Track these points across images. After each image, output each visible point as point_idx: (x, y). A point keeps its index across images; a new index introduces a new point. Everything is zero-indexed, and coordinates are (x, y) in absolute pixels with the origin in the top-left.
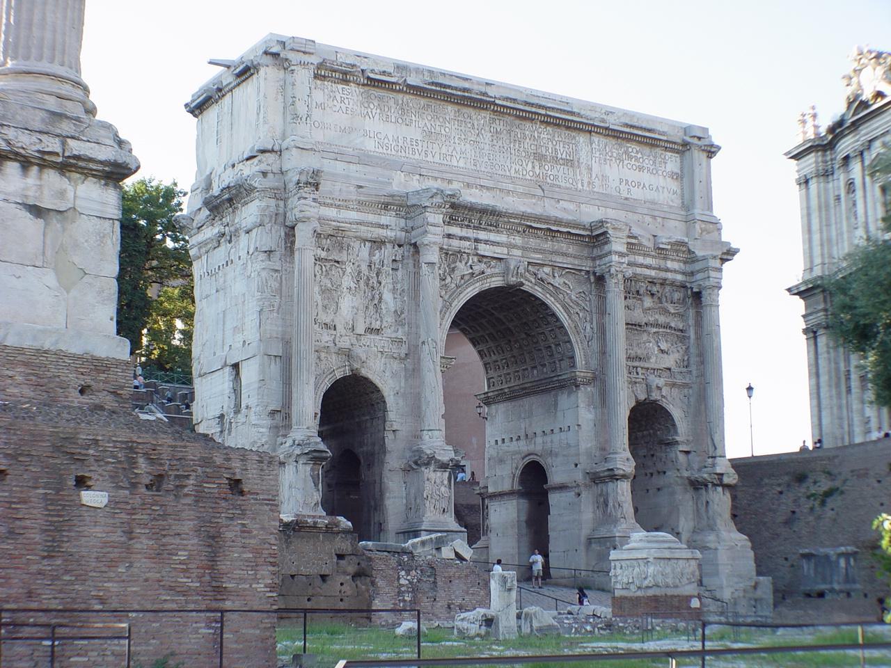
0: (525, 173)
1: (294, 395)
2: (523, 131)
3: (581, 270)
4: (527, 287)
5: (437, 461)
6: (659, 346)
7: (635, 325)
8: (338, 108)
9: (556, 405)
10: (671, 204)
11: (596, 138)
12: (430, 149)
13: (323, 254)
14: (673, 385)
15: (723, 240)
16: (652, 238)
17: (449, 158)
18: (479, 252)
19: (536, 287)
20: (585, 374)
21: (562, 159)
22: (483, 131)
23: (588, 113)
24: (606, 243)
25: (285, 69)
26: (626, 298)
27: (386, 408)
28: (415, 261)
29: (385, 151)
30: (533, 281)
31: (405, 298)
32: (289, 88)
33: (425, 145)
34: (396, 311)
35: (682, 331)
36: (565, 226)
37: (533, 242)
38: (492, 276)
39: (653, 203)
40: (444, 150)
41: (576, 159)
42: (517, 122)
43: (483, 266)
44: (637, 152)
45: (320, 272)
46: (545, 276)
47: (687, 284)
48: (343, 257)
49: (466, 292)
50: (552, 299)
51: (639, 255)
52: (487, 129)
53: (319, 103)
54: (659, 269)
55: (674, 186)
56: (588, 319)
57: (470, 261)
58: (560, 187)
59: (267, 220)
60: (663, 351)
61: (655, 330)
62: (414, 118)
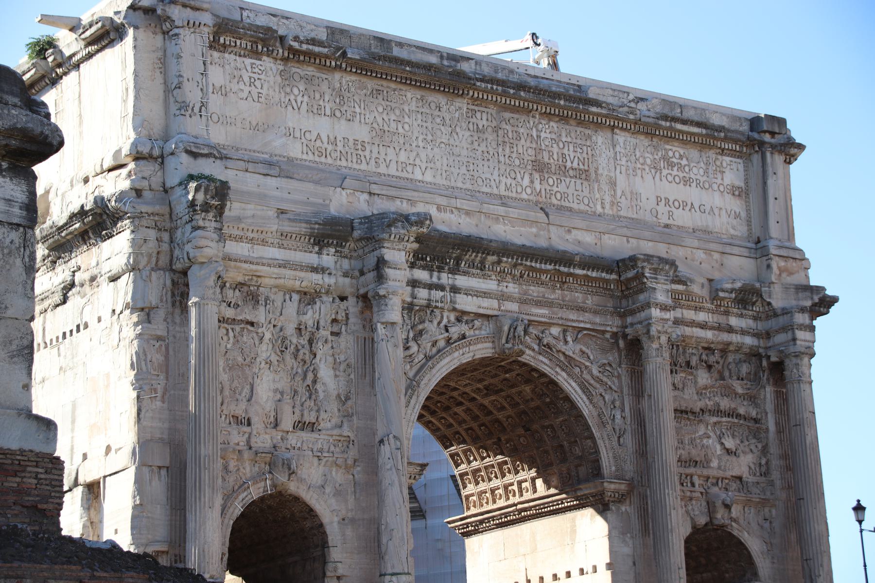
0: (519, 190)
1: (191, 526)
2: (515, 129)
3: (604, 332)
4: (528, 357)
6: (722, 444)
7: (686, 413)
9: (574, 531)
10: (732, 232)
11: (621, 137)
12: (382, 156)
13: (230, 313)
14: (747, 503)
15: (812, 283)
16: (706, 283)
17: (409, 169)
18: (457, 306)
19: (541, 358)
20: (617, 486)
22: (458, 129)
23: (610, 100)
24: (642, 291)
25: (164, 33)
26: (672, 372)
27: (327, 542)
28: (365, 320)
29: (317, 159)
30: (536, 347)
31: (352, 376)
32: (172, 62)
33: (375, 149)
34: (339, 396)
35: (756, 421)
36: (584, 265)
37: (535, 291)
38: (479, 340)
39: (707, 232)
40: (403, 157)
41: (592, 171)
42: (507, 115)
43: (464, 328)
44: (681, 157)
46: (553, 342)
47: (761, 351)
48: (260, 315)
50: (564, 374)
51: (689, 308)
52: (464, 125)
53: (217, 85)
55: (736, 205)
56: (617, 404)
57: (445, 321)
58: (570, 210)
59: (143, 262)
60: (728, 452)
61: (714, 419)
62: (357, 110)
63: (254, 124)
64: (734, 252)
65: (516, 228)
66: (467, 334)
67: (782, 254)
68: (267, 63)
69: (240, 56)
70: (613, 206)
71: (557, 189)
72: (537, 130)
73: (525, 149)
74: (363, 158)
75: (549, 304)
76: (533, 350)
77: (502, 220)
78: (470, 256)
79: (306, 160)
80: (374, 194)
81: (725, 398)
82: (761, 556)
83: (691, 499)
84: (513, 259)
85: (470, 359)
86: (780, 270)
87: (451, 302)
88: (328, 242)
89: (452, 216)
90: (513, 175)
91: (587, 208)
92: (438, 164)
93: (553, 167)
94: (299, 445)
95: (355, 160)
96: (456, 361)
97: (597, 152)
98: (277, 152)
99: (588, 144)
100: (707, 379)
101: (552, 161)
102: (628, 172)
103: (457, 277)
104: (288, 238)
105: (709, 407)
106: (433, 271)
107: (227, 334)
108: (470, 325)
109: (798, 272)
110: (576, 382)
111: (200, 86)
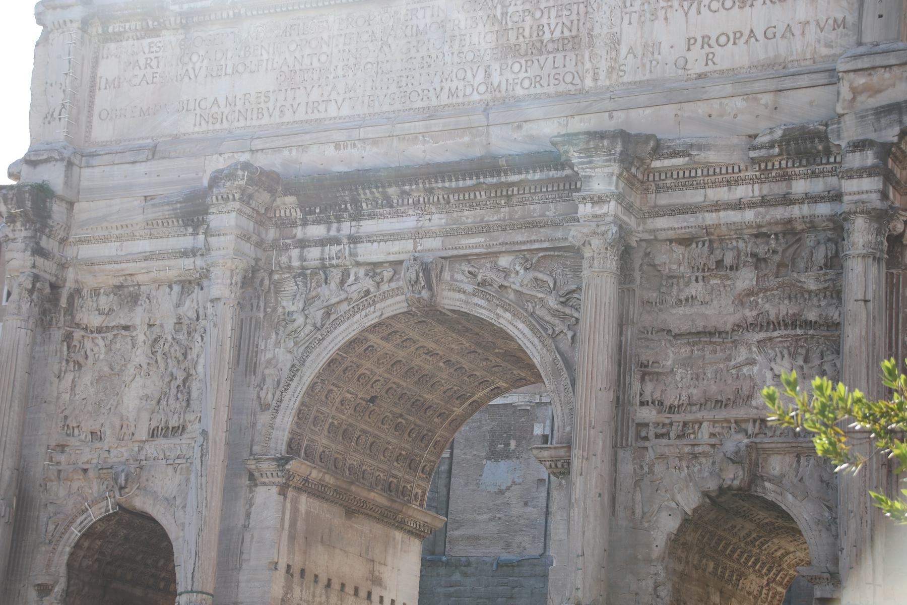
0: (469, 90)
6: (772, 369)
7: (711, 334)
10: (824, 51)
18: (359, 259)
19: (476, 300)
21: (552, 41)
29: (211, 127)
30: (469, 288)
37: (469, 217)
38: (385, 297)
41: (583, 33)
48: (138, 317)
49: (332, 336)
50: (508, 315)
51: (715, 184)
54: (764, 202)
57: (352, 278)
61: (762, 335)
62: (265, 56)
64: (799, 84)
65: (441, 143)
66: (372, 290)
67: (860, 66)
69: (138, 39)
70: (611, 73)
71: (526, 75)
72: (503, 6)
74: (265, 112)
76: (464, 292)
77: (421, 138)
78: (365, 195)
79: (197, 132)
80: (257, 151)
81: (786, 302)
83: (695, 456)
84: (417, 184)
85: (377, 320)
86: (854, 93)
87: (350, 254)
88: (198, 219)
89: (356, 149)
90: (461, 75)
91: (570, 87)
93: (523, 46)
94: (155, 454)
95: (255, 116)
96: (356, 325)
97: (595, 6)
100: (752, 280)
101: (521, 39)
102: (643, 19)
103: (362, 223)
104: (155, 226)
105: (750, 320)
106: (331, 222)
108: (378, 279)
109: (894, 85)
110: (524, 322)
111: (63, 87)
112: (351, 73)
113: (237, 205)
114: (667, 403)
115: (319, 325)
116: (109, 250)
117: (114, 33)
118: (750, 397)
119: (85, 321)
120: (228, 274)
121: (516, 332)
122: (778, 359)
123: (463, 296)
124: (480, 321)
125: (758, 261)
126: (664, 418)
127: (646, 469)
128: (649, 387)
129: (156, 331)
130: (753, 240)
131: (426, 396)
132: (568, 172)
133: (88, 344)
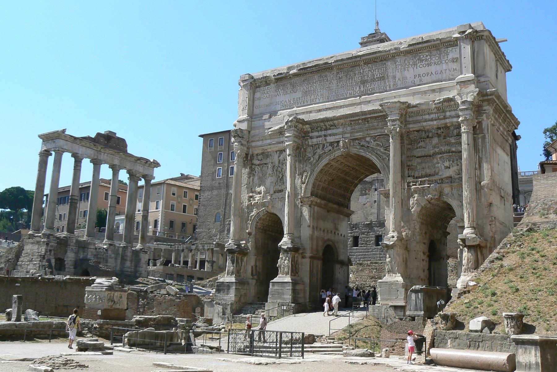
5: (283, 248)
7: (427, 156)
8: (266, 95)
12: (306, 99)
19: (360, 150)
30: (358, 147)
38: (335, 151)
40: (312, 97)
41: (385, 75)
42: (351, 69)
43: (330, 148)
44: (427, 56)
45: (258, 170)
48: (268, 161)
49: (321, 163)
50: (370, 154)
51: (425, 115)
52: (335, 79)
57: (326, 146)
62: (298, 88)
63: (267, 104)
66: (331, 149)
68: (272, 85)
73: (358, 78)
75: (363, 131)
81: (447, 146)
82: (457, 207)
83: (424, 190)
87: (325, 140)
90: (353, 88)
92: (325, 95)
98: (273, 110)
99: (384, 66)
103: (327, 131)
105: (437, 152)
107: (258, 169)
108: (333, 146)
112: (322, 91)
113: (293, 128)
114: (415, 176)
115: (317, 160)
116: (260, 143)
117: (259, 86)
118: (438, 173)
119: (255, 163)
120: (292, 147)
121: (372, 158)
122: (445, 162)
123: (357, 150)
124: (362, 156)
125: (439, 136)
126: (415, 180)
127: (410, 194)
128: (410, 172)
129: (274, 164)
130: (436, 129)
131: (348, 178)
132: (384, 113)
133: (256, 169)
